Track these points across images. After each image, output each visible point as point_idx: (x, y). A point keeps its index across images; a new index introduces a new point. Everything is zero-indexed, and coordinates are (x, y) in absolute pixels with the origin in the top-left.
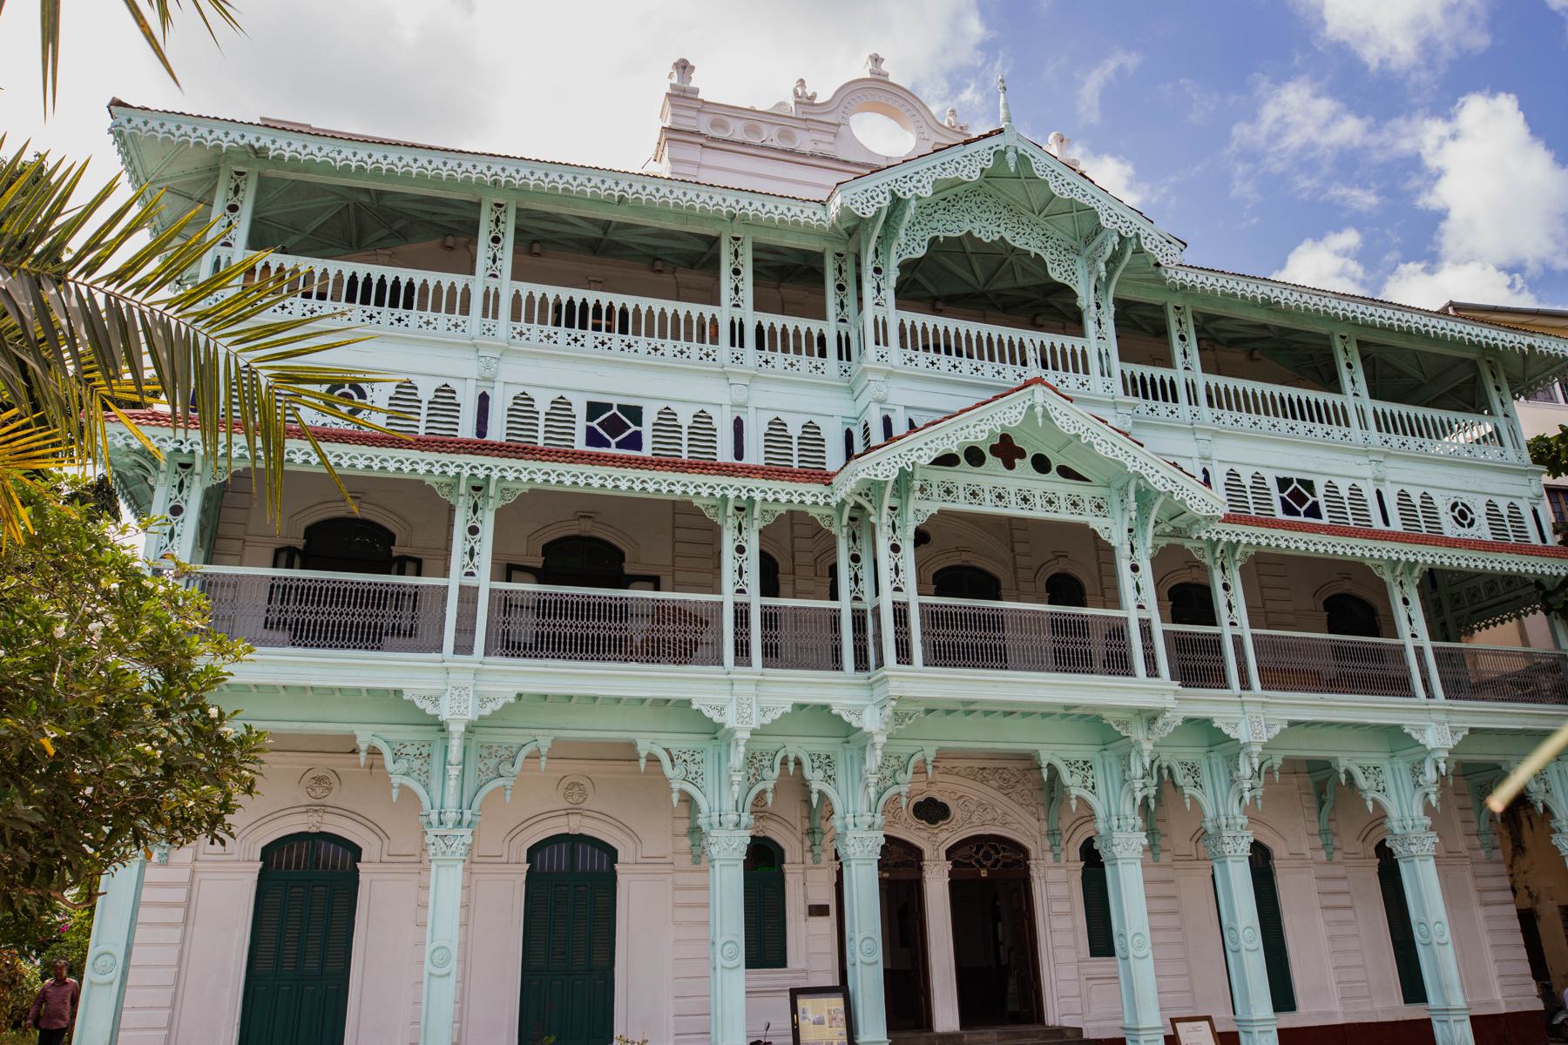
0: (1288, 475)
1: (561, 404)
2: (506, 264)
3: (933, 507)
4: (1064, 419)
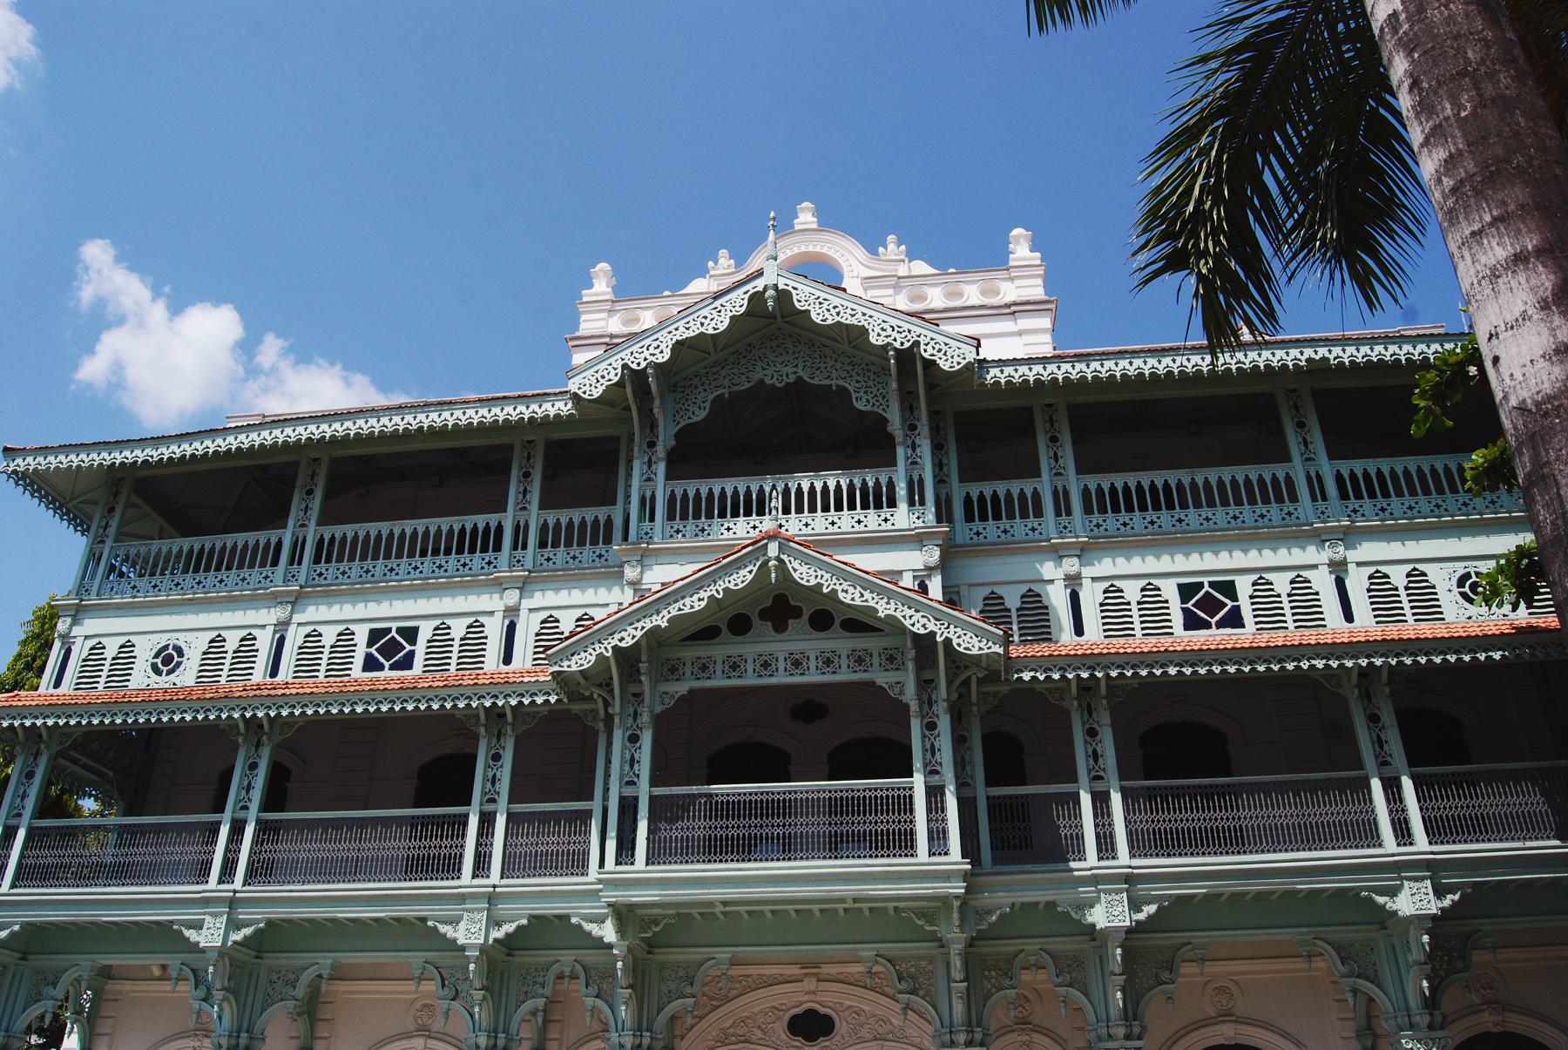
1: (346, 635)
3: (681, 688)
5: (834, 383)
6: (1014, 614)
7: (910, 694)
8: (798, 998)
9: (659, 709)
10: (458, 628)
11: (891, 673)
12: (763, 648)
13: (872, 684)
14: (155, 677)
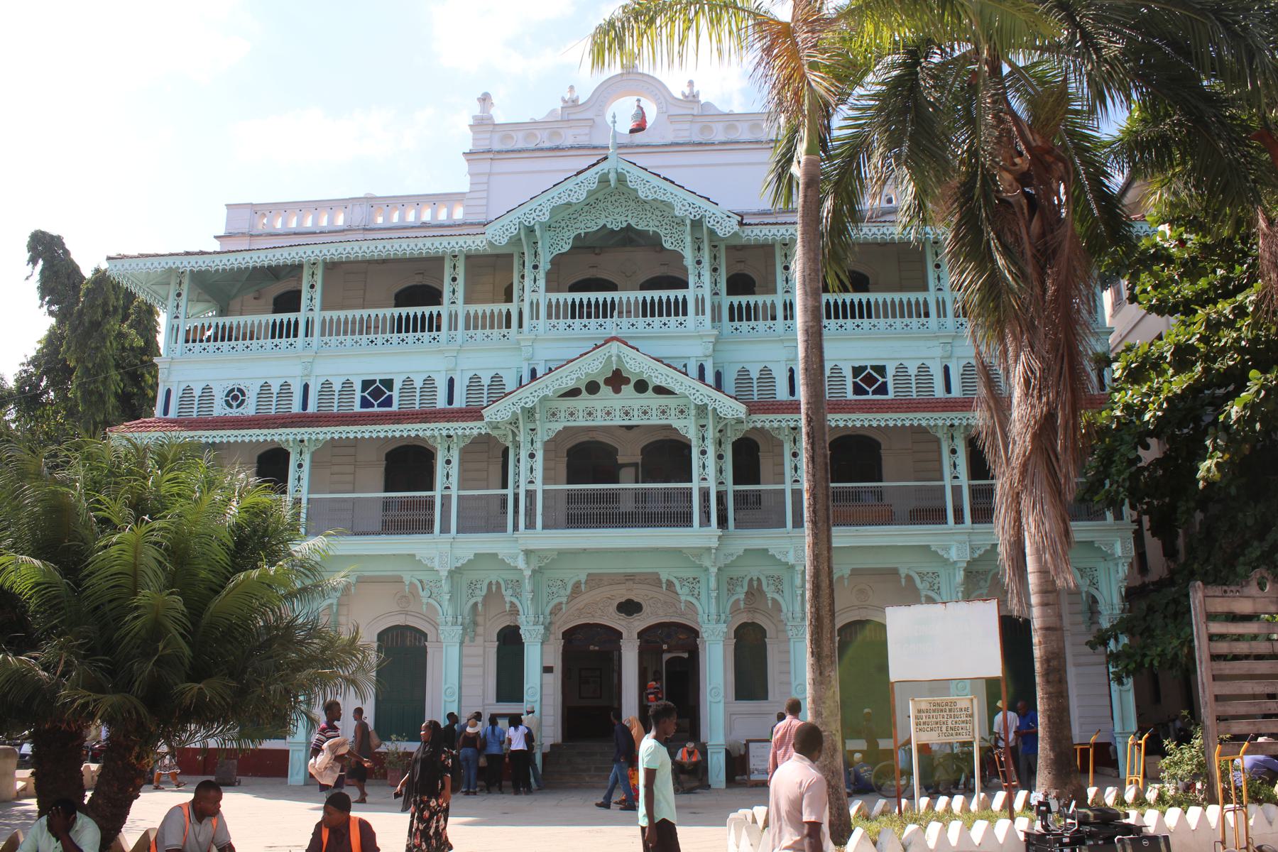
0: (863, 364)
1: (347, 384)
3: (559, 426)
4: (632, 362)
5: (651, 229)
6: (755, 381)
8: (622, 594)
9: (546, 438)
12: (608, 403)
14: (228, 410)
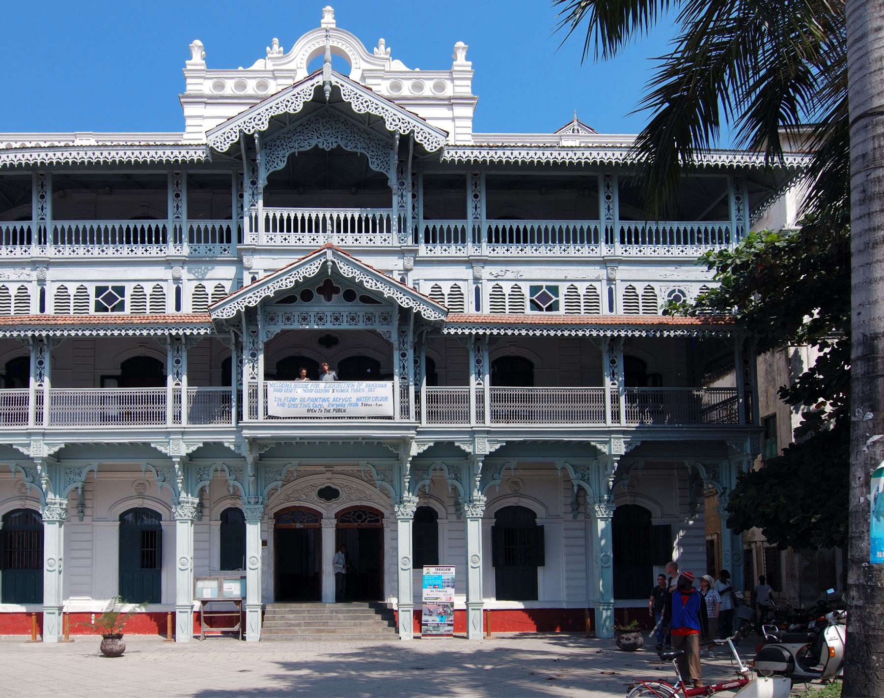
1: (82, 290)
2: (48, 211)
5: (359, 151)
7: (394, 338)
8: (323, 481)
10: (148, 289)
11: (385, 326)
13: (374, 332)
